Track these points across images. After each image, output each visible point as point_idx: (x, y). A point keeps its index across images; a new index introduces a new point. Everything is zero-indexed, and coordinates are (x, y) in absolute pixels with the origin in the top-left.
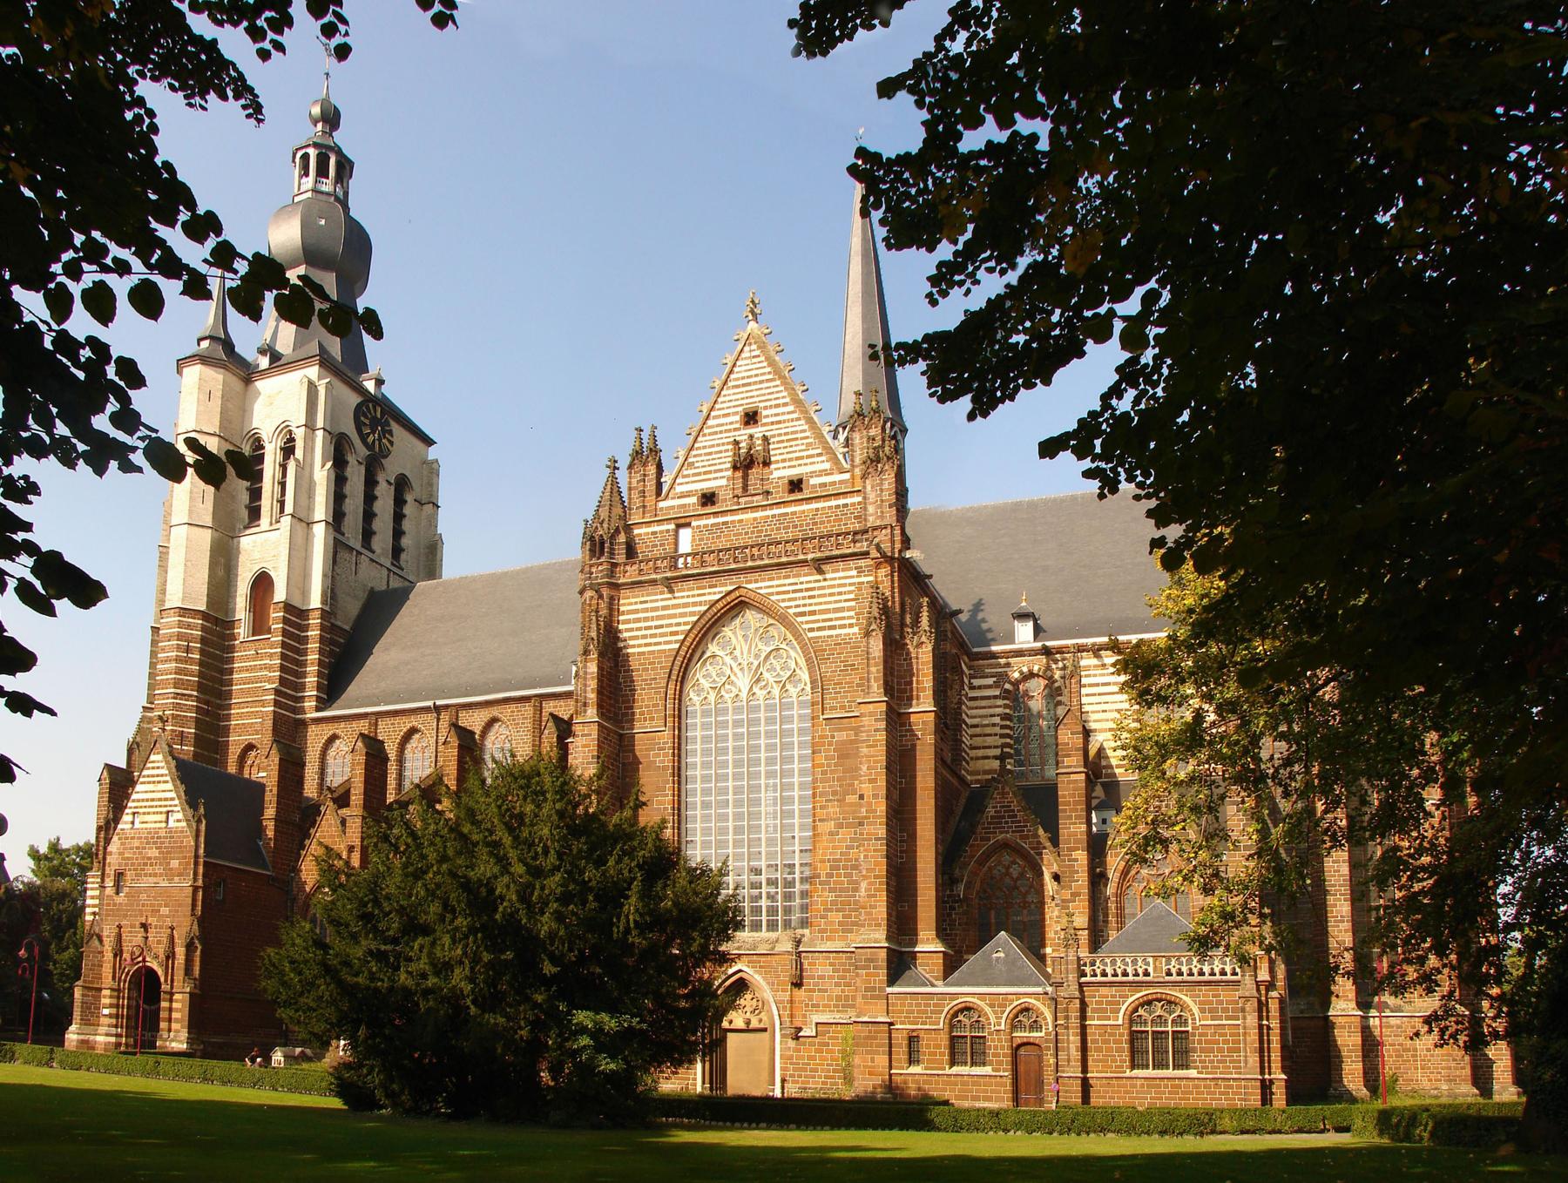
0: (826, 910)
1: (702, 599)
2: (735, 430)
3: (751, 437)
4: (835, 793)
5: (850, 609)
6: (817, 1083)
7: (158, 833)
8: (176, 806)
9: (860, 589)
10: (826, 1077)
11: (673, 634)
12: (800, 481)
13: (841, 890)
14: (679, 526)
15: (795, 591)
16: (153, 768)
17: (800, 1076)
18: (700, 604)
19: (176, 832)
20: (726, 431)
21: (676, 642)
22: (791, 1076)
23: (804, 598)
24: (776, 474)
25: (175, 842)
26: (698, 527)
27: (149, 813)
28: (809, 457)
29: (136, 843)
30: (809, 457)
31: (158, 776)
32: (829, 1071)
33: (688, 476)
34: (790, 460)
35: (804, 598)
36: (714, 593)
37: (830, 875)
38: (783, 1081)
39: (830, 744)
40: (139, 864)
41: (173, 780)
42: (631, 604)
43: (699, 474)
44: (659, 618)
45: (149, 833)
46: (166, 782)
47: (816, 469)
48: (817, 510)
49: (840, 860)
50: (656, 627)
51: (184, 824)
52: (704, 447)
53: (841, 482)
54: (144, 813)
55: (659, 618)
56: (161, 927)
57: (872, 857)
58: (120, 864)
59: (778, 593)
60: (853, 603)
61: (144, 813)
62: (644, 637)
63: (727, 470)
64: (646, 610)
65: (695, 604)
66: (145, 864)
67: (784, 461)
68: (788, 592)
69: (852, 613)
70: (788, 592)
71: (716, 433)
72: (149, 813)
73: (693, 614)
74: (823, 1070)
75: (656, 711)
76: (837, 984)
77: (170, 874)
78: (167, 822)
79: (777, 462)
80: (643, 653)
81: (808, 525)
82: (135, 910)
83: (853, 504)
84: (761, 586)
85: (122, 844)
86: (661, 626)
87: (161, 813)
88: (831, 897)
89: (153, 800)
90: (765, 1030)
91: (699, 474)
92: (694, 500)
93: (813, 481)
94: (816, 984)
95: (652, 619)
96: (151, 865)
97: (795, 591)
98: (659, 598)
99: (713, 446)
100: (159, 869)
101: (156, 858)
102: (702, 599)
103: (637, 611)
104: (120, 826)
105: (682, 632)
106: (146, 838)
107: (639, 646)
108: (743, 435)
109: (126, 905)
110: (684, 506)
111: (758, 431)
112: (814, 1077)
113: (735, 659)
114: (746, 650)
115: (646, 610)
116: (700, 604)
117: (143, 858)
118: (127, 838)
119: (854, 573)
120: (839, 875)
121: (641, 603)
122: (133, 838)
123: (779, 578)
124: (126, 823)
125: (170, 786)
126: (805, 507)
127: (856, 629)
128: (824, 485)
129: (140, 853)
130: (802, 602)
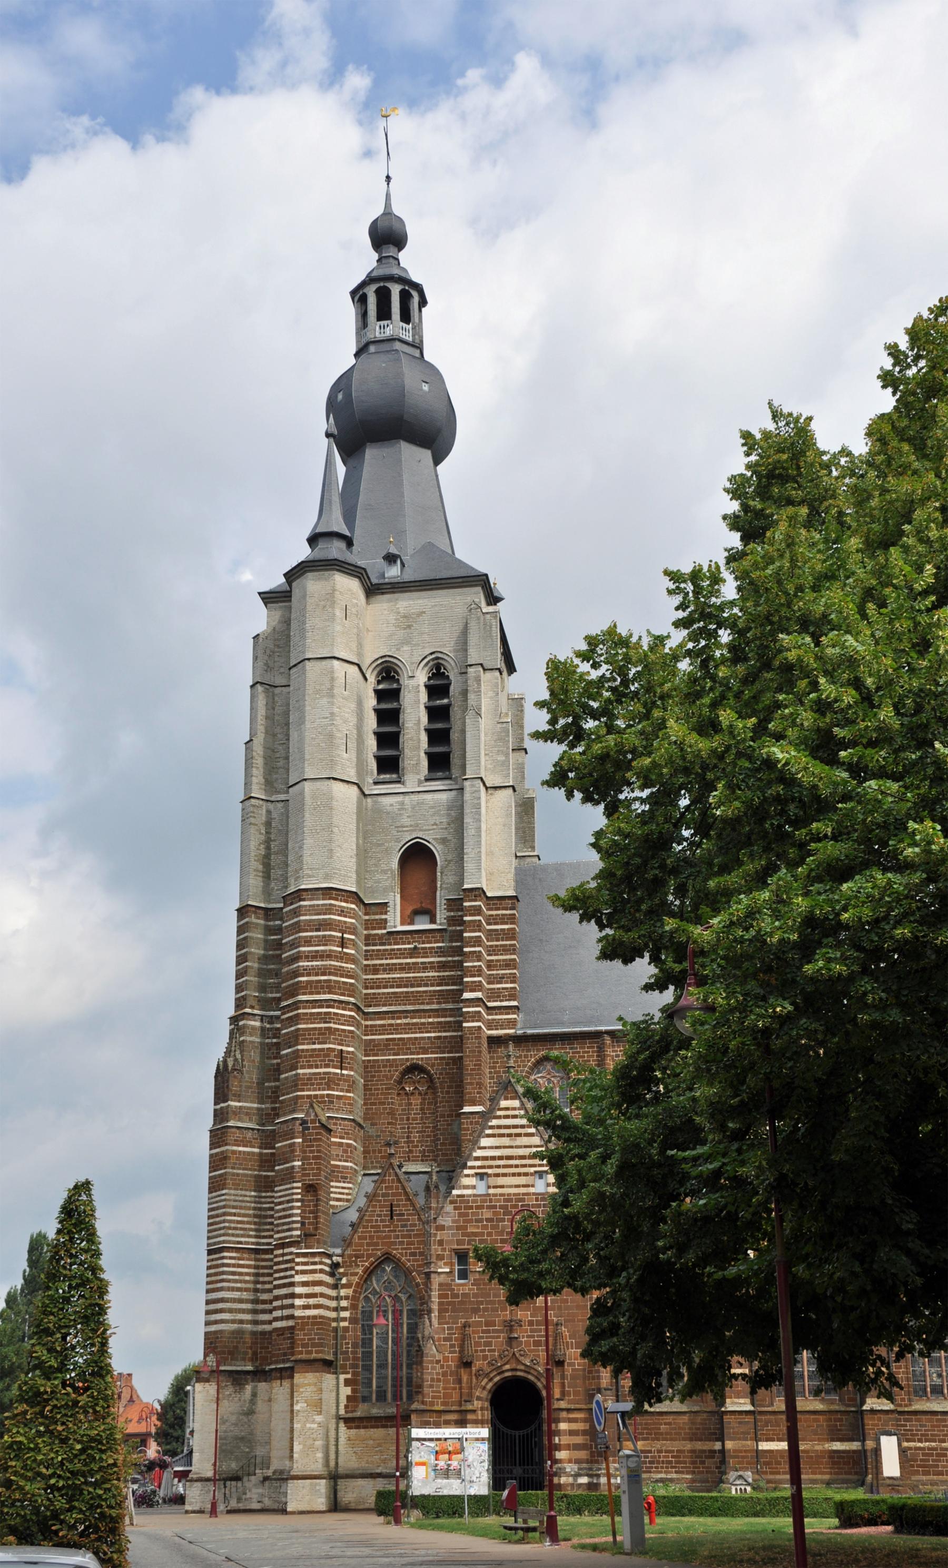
7: (523, 1200)
16: (507, 1117)
29: (487, 1214)
45: (506, 1200)
46: (532, 1135)
54: (497, 1175)
58: (459, 1242)
61: (497, 1175)
72: (505, 1175)
82: (493, 1302)
85: (460, 1215)
87: (526, 1174)
104: (455, 1192)
109: (475, 1295)
129: (493, 1227)
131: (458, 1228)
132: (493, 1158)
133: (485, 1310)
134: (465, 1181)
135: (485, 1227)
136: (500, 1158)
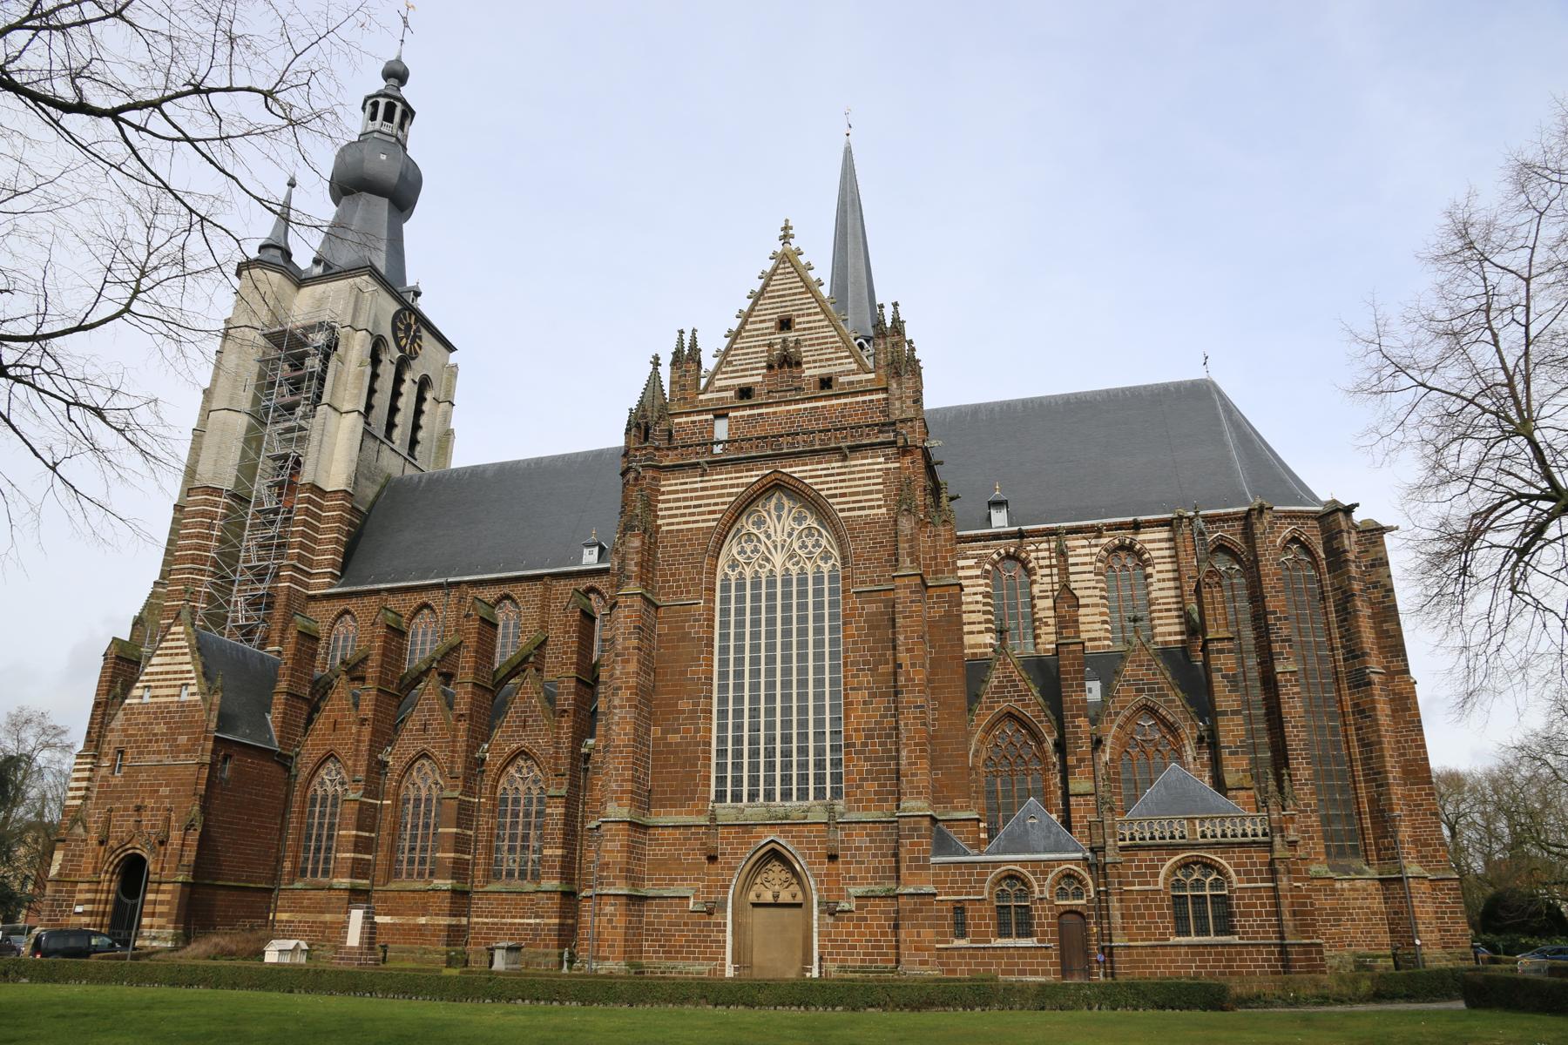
0: (862, 779)
1: (740, 481)
2: (771, 334)
3: (785, 340)
4: (866, 663)
5: (878, 492)
6: (856, 960)
7: (167, 707)
8: (192, 678)
9: (887, 474)
10: (865, 954)
11: (711, 512)
12: (830, 379)
13: (876, 759)
14: (717, 417)
15: (826, 476)
16: (173, 640)
17: (838, 954)
18: (738, 486)
19: (188, 706)
20: (762, 335)
21: (714, 520)
22: (830, 954)
23: (835, 482)
24: (808, 373)
25: (186, 717)
26: (735, 417)
27: (161, 687)
28: (837, 358)
29: (142, 719)
30: (837, 358)
31: (177, 648)
32: (867, 947)
33: (726, 373)
34: (821, 361)
35: (835, 482)
36: (752, 477)
37: (865, 745)
38: (821, 959)
39: (860, 615)
40: (143, 741)
41: (193, 653)
42: (671, 485)
43: (736, 371)
44: (698, 498)
45: (159, 708)
46: (185, 654)
47: (843, 367)
48: (845, 404)
49: (874, 729)
50: (695, 507)
51: (198, 698)
52: (742, 348)
53: (867, 381)
54: (156, 687)
55: (698, 498)
56: (158, 809)
57: (912, 724)
59: (811, 477)
60: (881, 487)
61: (156, 687)
62: (683, 515)
63: (762, 368)
64: (685, 491)
65: (732, 486)
66: (150, 741)
67: (815, 361)
68: (820, 476)
69: (881, 496)
70: (820, 476)
71: (753, 336)
72: (161, 687)
73: (730, 495)
74: (861, 947)
75: (693, 585)
76: (875, 856)
77: (175, 750)
78: (179, 696)
79: (809, 362)
80: (682, 530)
81: (837, 417)
83: (878, 400)
84: (796, 470)
85: (127, 720)
86: (700, 506)
87: (175, 686)
88: (866, 766)
89: (167, 673)
90: (799, 905)
91: (736, 371)
92: (732, 393)
93: (841, 380)
94: (854, 856)
95: (692, 499)
96: (157, 741)
97: (826, 476)
98: (695, 482)
99: (750, 347)
100: (164, 746)
101: (163, 734)
102: (740, 481)
103: (677, 492)
105: (720, 511)
106: (155, 713)
107: (678, 523)
108: (778, 337)
109: (122, 786)
110: (722, 399)
111: (791, 336)
112: (852, 954)
113: (769, 537)
114: (779, 529)
115: (685, 491)
116: (738, 486)
117: (148, 735)
118: (133, 714)
119: (882, 460)
120: (874, 744)
121: (682, 484)
122: (140, 713)
123: (812, 464)
124: (135, 697)
125: (188, 658)
126: (834, 402)
127: (884, 510)
128: (851, 383)
129: (146, 729)
130: (833, 485)
131: (123, 730)
132: (157, 673)
133: (125, 798)
134: (136, 692)
135: (140, 729)
136: (161, 673)
